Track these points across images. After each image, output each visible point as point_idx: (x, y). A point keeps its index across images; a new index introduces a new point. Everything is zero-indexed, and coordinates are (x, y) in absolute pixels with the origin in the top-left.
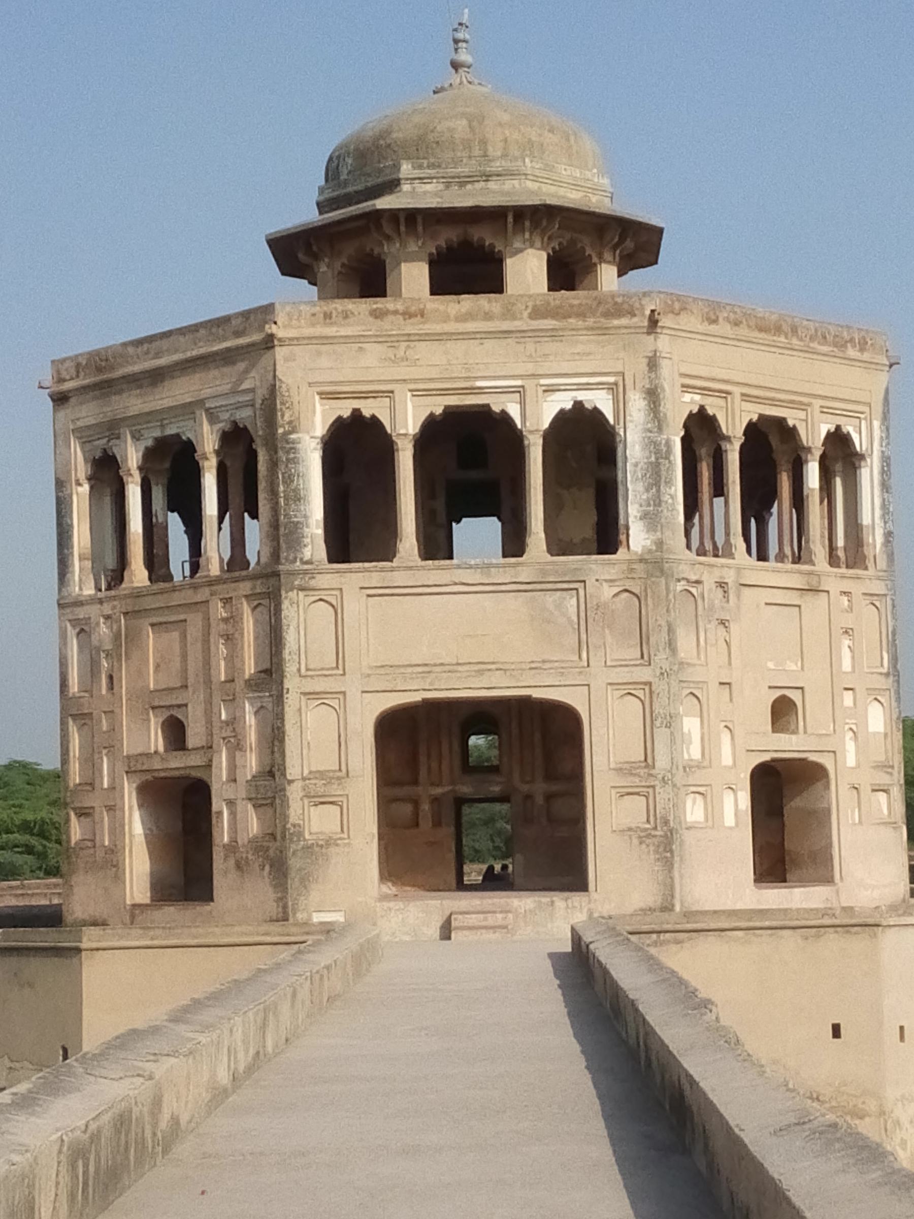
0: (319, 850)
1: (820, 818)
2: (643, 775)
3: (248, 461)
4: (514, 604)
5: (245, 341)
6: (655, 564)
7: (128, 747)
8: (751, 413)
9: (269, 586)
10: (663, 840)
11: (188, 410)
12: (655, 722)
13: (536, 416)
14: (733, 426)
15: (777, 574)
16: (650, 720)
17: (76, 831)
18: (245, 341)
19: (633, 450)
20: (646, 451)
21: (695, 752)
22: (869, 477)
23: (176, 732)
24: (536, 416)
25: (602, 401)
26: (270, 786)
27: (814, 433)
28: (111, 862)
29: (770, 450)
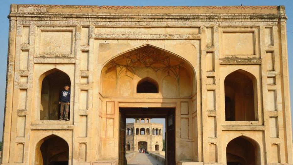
0: (135, 148)
1: (159, 147)
2: (150, 145)
3: (132, 130)
6: (151, 135)
8: (156, 128)
9: (133, 136)
10: (151, 148)
11: (129, 127)
12: (151, 143)
13: (146, 128)
14: (155, 129)
15: (157, 136)
16: (150, 143)
20: (151, 130)
21: (152, 144)
22: (162, 131)
24: (146, 128)
25: (149, 128)
26: (133, 145)
27: (159, 129)
29: (157, 130)
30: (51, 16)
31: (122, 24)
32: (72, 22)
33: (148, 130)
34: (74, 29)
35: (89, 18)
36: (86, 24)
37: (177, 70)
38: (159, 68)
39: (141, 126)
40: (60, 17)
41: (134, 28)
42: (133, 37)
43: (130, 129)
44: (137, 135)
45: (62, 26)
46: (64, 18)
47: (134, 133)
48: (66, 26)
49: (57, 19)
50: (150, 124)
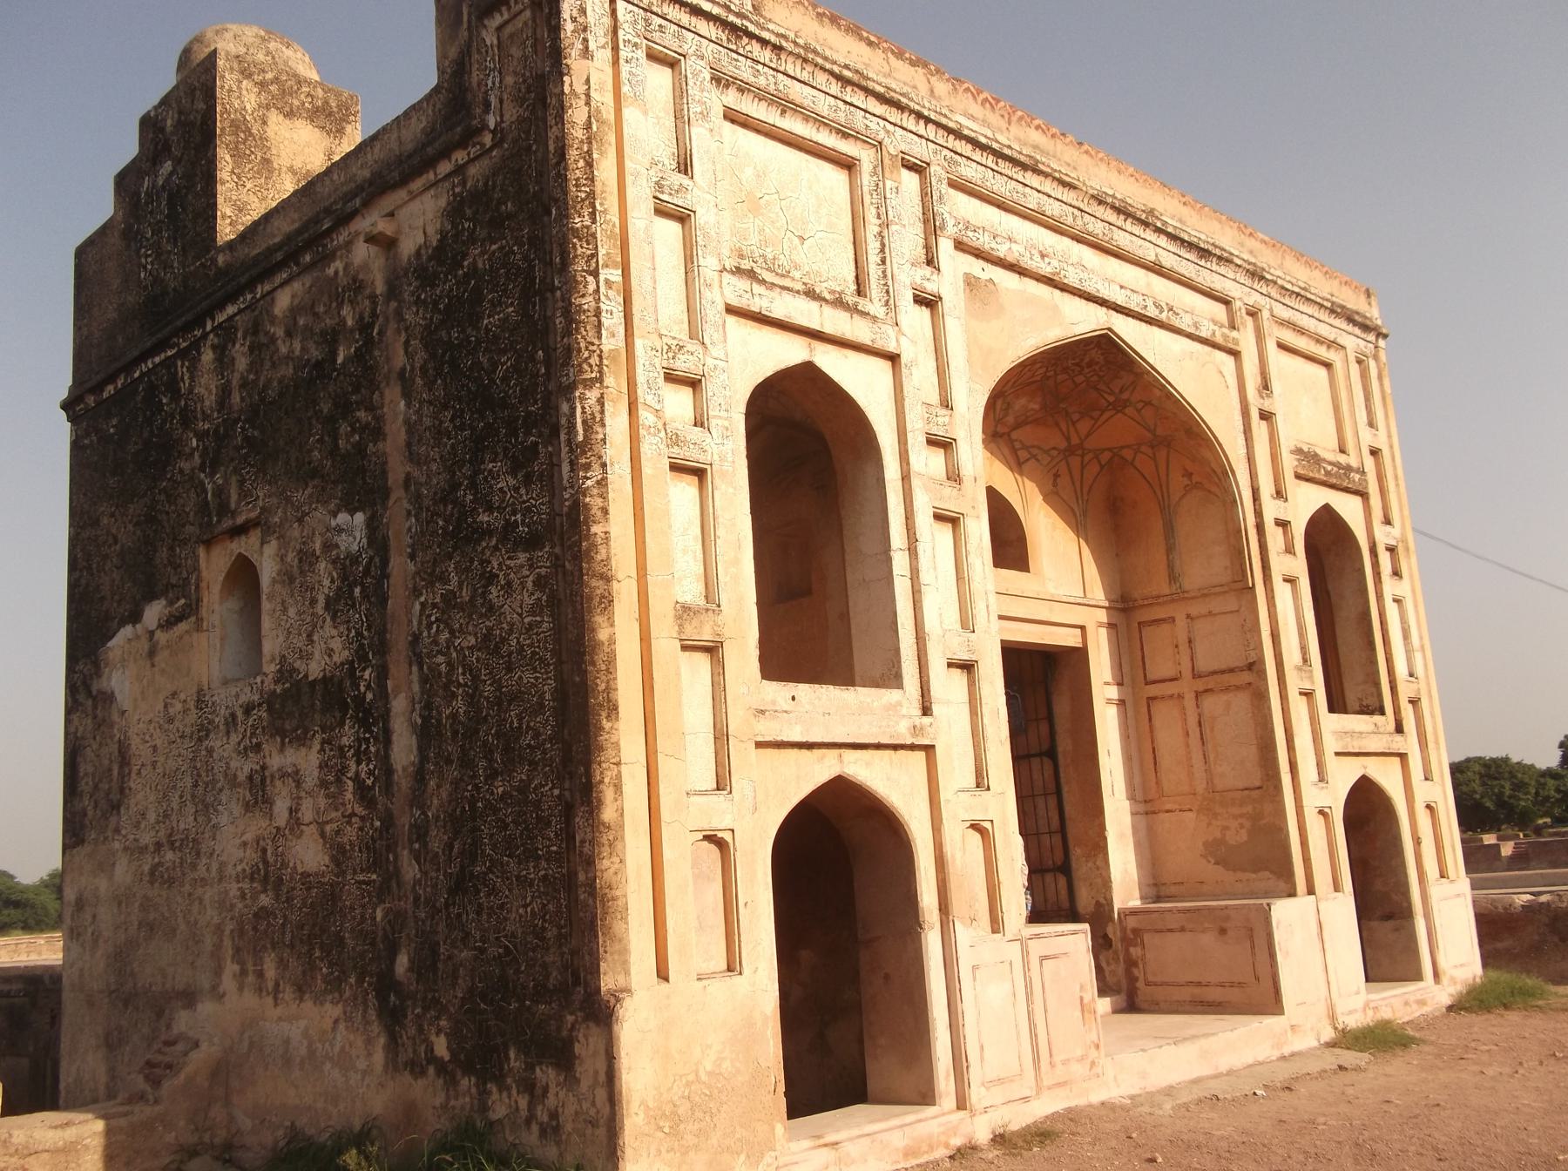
30: (784, 44)
31: (1032, 201)
32: (870, 117)
34: (866, 157)
35: (928, 120)
36: (920, 150)
37: (1093, 469)
38: (1035, 451)
40: (823, 69)
41: (1062, 233)
42: (1072, 279)
45: (820, 121)
46: (833, 81)
48: (838, 131)
49: (805, 76)
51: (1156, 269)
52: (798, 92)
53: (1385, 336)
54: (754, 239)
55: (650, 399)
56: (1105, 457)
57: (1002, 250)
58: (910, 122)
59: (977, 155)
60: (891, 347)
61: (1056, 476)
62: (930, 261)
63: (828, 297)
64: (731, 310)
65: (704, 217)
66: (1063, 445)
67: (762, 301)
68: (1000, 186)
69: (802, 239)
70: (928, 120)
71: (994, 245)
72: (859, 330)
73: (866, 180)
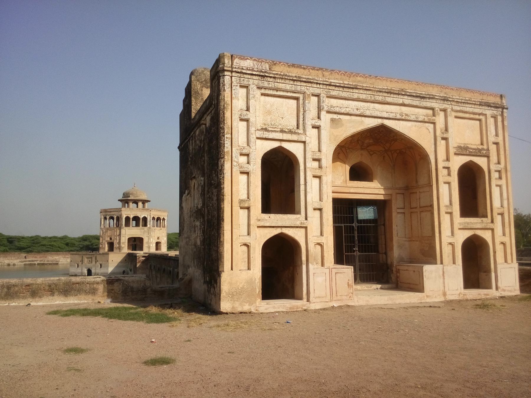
3: (118, 219)
4: (139, 230)
5: (119, 210)
6: (150, 228)
7: (106, 239)
13: (141, 217)
14: (156, 218)
17: (101, 246)
18: (119, 210)
19: (148, 219)
23: (111, 239)
24: (141, 217)
26: (119, 243)
27: (162, 218)
28: (104, 248)
29: (159, 219)
33: (145, 219)
39: (134, 213)
43: (115, 217)
44: (127, 228)
47: (122, 225)
50: (148, 209)
51: (403, 105)
52: (281, 86)
53: (507, 109)
54: (269, 120)
55: (235, 160)
56: (398, 151)
57: (343, 111)
58: (315, 86)
59: (337, 89)
60: (303, 140)
61: (384, 157)
62: (319, 118)
63: (287, 130)
64: (258, 138)
65: (252, 120)
66: (383, 150)
67: (267, 135)
68: (344, 94)
69: (282, 118)
70: (320, 84)
71: (340, 110)
72: (295, 137)
73: (301, 101)
